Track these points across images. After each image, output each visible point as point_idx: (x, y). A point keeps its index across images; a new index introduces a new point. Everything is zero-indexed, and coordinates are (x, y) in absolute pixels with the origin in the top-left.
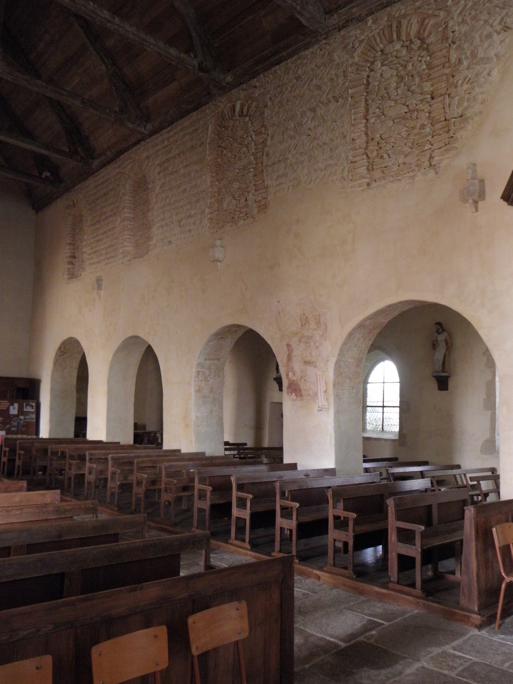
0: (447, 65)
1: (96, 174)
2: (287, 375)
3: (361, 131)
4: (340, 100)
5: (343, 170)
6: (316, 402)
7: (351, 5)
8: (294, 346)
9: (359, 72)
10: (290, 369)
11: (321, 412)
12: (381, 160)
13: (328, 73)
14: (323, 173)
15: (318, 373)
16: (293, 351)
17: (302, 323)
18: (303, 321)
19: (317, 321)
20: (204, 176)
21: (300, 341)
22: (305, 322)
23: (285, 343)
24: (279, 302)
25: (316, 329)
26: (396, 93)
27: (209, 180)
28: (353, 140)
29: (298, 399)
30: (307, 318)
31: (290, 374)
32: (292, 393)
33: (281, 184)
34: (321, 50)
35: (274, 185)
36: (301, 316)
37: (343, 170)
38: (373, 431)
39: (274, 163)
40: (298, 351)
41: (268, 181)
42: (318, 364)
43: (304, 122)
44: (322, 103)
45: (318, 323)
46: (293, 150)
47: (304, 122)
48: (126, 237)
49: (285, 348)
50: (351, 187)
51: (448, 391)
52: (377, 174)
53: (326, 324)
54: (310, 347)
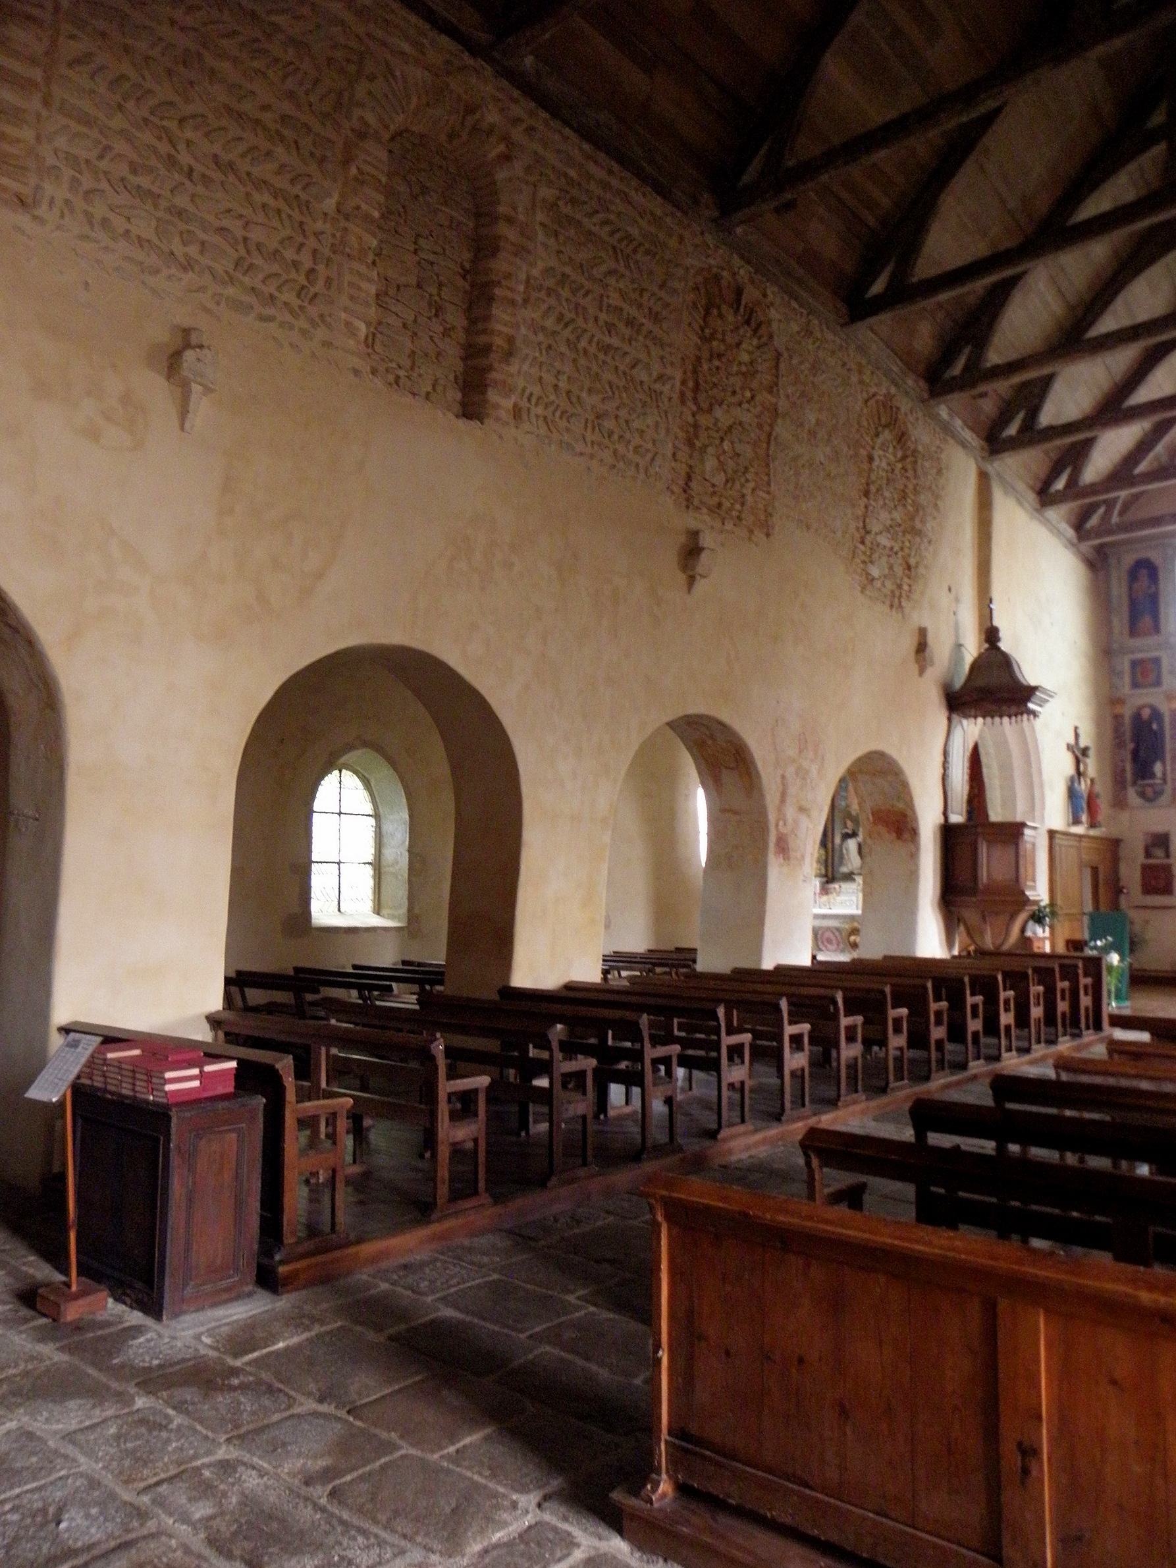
2: (777, 825)
10: (782, 817)
23: (780, 772)
31: (781, 823)
49: (778, 780)
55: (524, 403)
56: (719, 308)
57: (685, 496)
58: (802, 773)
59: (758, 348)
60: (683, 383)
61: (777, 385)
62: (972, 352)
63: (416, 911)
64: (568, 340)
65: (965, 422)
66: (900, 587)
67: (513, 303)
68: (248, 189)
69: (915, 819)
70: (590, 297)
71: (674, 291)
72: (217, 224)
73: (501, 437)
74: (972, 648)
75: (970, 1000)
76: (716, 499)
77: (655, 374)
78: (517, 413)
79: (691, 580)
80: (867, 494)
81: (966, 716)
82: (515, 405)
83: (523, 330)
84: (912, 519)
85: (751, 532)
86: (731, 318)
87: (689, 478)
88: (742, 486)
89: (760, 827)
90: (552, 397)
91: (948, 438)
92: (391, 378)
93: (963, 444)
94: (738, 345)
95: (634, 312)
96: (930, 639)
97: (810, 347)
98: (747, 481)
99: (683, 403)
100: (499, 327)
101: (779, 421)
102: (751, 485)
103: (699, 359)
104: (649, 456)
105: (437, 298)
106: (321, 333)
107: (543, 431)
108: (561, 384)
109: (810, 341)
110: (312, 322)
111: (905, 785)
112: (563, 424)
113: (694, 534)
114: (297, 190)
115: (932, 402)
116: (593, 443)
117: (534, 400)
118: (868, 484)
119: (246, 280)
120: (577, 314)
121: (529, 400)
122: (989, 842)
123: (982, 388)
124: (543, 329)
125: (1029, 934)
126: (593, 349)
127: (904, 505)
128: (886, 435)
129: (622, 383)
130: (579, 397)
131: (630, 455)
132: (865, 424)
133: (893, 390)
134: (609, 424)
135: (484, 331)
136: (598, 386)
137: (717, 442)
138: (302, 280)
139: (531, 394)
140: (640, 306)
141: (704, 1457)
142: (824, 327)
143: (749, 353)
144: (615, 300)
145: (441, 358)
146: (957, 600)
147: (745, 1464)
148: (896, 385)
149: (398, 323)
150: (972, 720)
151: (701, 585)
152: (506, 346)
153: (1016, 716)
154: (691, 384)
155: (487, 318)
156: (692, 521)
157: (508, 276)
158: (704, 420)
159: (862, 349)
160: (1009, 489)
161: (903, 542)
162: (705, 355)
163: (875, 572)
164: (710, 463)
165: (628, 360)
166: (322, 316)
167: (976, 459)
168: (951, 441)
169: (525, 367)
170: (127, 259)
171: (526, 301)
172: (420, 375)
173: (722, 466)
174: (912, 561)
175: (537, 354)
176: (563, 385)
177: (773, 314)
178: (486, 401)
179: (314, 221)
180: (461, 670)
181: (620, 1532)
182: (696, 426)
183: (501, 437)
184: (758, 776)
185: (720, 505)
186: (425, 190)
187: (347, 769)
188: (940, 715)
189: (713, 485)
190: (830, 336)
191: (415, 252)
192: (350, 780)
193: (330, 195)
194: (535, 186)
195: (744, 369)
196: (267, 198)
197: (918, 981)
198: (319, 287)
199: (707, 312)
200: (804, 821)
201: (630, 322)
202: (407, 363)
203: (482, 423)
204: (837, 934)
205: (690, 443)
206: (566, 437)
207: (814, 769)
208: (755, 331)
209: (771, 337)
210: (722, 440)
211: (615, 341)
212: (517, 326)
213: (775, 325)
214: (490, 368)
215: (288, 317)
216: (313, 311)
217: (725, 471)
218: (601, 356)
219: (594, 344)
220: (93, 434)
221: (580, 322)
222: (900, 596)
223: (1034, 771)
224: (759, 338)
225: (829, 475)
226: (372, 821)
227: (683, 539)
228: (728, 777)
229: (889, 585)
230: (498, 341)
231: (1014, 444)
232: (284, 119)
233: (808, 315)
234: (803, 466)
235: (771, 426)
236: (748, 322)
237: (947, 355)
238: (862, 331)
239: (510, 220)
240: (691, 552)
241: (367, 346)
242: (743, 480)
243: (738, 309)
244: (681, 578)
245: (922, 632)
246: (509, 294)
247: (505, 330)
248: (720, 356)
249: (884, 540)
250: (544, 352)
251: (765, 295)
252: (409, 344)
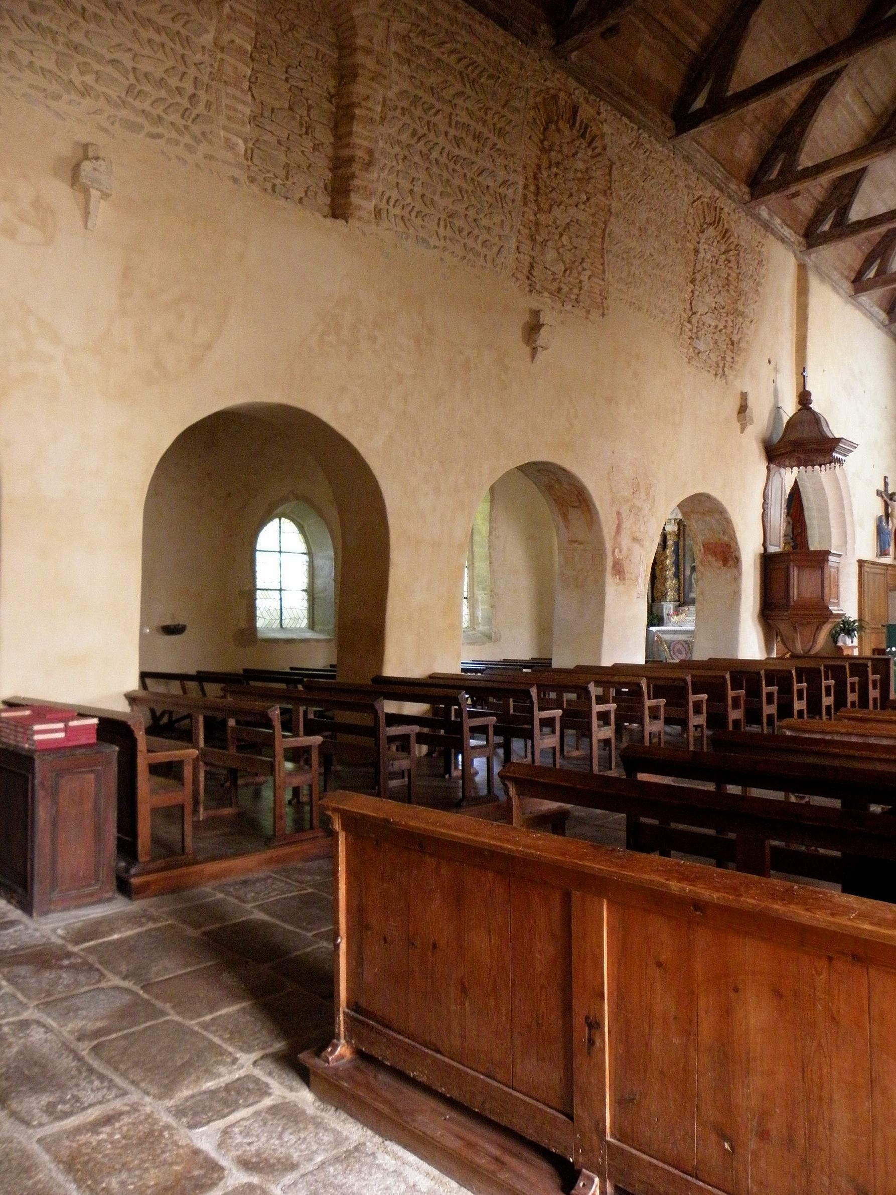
2: (613, 552)
8: (624, 515)
10: (617, 545)
23: (615, 509)
45: (648, 494)
49: (615, 515)
55: (383, 205)
56: (557, 122)
57: (527, 282)
58: (636, 511)
59: (593, 157)
60: (526, 187)
61: (610, 188)
62: (785, 158)
64: (421, 152)
65: (784, 222)
66: (724, 358)
68: (135, 27)
69: (738, 549)
70: (439, 116)
71: (517, 110)
72: (108, 56)
73: (364, 233)
74: (790, 408)
75: (765, 689)
76: (556, 285)
77: (500, 181)
78: (378, 213)
79: (534, 351)
80: (693, 281)
81: (785, 467)
82: (375, 207)
83: (381, 144)
84: (735, 302)
85: (588, 312)
86: (567, 132)
87: (532, 267)
88: (579, 274)
89: (599, 553)
90: (409, 200)
91: (768, 234)
92: (269, 186)
93: (783, 240)
94: (574, 155)
95: (479, 127)
96: (751, 402)
97: (641, 157)
98: (584, 269)
99: (525, 204)
100: (358, 141)
101: (612, 219)
102: (588, 273)
103: (539, 167)
104: (495, 249)
105: (307, 119)
106: (203, 148)
107: (401, 228)
108: (415, 189)
109: (641, 151)
110: (196, 139)
111: (728, 521)
112: (418, 222)
113: (536, 313)
114: (178, 26)
115: (753, 203)
116: (445, 238)
117: (391, 204)
118: (694, 273)
119: (137, 104)
120: (429, 129)
121: (388, 202)
122: (800, 568)
123: (794, 189)
124: (399, 142)
125: (840, 644)
126: (443, 159)
127: (728, 291)
128: (711, 232)
129: (470, 188)
130: (432, 200)
131: (479, 248)
132: (691, 221)
133: (717, 193)
134: (459, 222)
135: (348, 145)
136: (449, 190)
137: (557, 237)
138: (186, 103)
139: (390, 197)
140: (485, 122)
141: (369, 1025)
142: (652, 139)
143: (585, 161)
144: (464, 118)
145: (311, 169)
146: (776, 370)
147: (395, 1032)
148: (721, 190)
149: (274, 140)
150: (789, 469)
151: (541, 356)
152: (367, 158)
153: (825, 464)
154: (532, 188)
155: (350, 133)
156: (534, 303)
157: (367, 98)
158: (543, 218)
159: (688, 159)
160: (824, 277)
161: (726, 321)
162: (545, 163)
163: (701, 346)
164: (550, 256)
165: (475, 168)
167: (794, 252)
168: (771, 237)
169: (384, 174)
170: (32, 86)
171: (383, 119)
172: (294, 183)
173: (561, 258)
174: (735, 338)
175: (394, 164)
176: (418, 189)
177: (606, 128)
178: (350, 204)
179: (195, 54)
180: (333, 424)
181: (308, 1083)
182: (537, 224)
183: (364, 233)
184: (597, 513)
185: (559, 290)
186: (293, 27)
187: (286, 517)
188: (760, 465)
189: (554, 274)
190: (659, 147)
191: (287, 80)
192: (288, 525)
193: (207, 31)
194: (389, 21)
195: (579, 175)
196: (151, 34)
197: (719, 673)
198: (201, 108)
199: (546, 129)
200: (637, 548)
201: (477, 137)
202: (283, 173)
203: (347, 222)
204: (686, 646)
205: (534, 240)
206: (422, 234)
207: (646, 507)
208: (590, 144)
209: (604, 148)
210: (561, 235)
211: (464, 153)
212: (377, 142)
213: (607, 140)
214: (353, 176)
215: (174, 135)
216: (196, 129)
217: (564, 262)
218: (451, 165)
219: (445, 155)
221: (431, 136)
222: (724, 367)
223: (846, 511)
224: (593, 150)
225: (658, 265)
226: (306, 558)
227: (527, 317)
228: (574, 514)
229: (714, 357)
230: (359, 153)
231: (826, 238)
233: (639, 129)
234: (635, 257)
235: (605, 223)
236: (583, 136)
237: (766, 163)
238: (686, 141)
239: (368, 51)
240: (533, 328)
241: (247, 159)
242: (580, 268)
243: (574, 124)
244: (526, 350)
245: (744, 396)
246: (370, 114)
247: (365, 143)
248: (557, 165)
249: (709, 320)
250: (400, 162)
251: (599, 113)
252: (283, 159)
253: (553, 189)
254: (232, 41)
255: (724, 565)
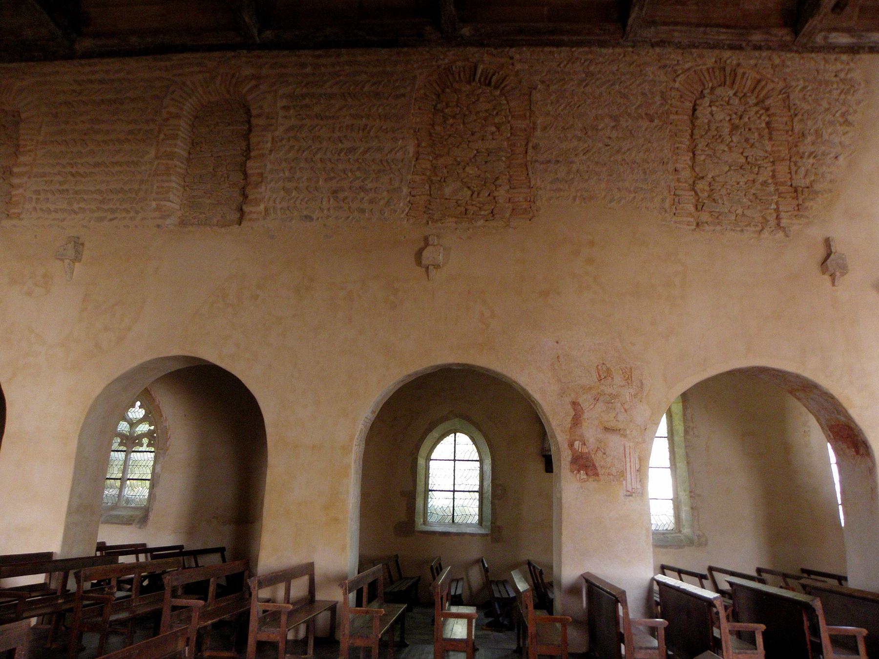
0: (790, 133)
1: (92, 61)
2: (571, 445)
3: (687, 164)
4: (656, 121)
5: (663, 200)
6: (622, 484)
7: (675, 28)
8: (585, 405)
9: (682, 100)
11: (630, 497)
12: (714, 204)
13: (639, 85)
14: (632, 195)
15: (627, 445)
16: (583, 413)
17: (600, 376)
18: (601, 373)
19: (627, 376)
20: (401, 141)
21: (597, 400)
22: (604, 374)
23: (567, 400)
24: (557, 342)
25: (624, 386)
26: (730, 140)
27: (411, 149)
28: (676, 170)
29: (590, 480)
30: (608, 370)
31: (577, 444)
32: (579, 471)
33: (559, 190)
34: (624, 56)
35: (548, 188)
36: (598, 366)
37: (663, 200)
38: (440, 523)
39: (549, 162)
40: (593, 414)
41: (536, 179)
42: (628, 432)
43: (600, 127)
44: (629, 115)
46: (582, 155)
47: (600, 127)
48: (174, 185)
49: (569, 407)
50: (675, 222)
51: (544, 473)
52: (705, 216)
53: (641, 381)
54: (615, 409)
63: (498, 523)
67: (263, 155)
96: (836, 247)
101: (538, 133)
116: (329, 209)
119: (106, 207)
166: (141, 208)
170: (54, 219)
191: (212, 156)
192: (463, 439)
193: (148, 153)
196: (118, 168)
207: (627, 394)
212: (266, 165)
215: (124, 215)
220: (29, 294)
226: (478, 463)
232: (131, 132)
239: (259, 116)
245: (828, 242)
247: (257, 171)
253: (450, 136)
254: (165, 151)
255: (857, 452)
